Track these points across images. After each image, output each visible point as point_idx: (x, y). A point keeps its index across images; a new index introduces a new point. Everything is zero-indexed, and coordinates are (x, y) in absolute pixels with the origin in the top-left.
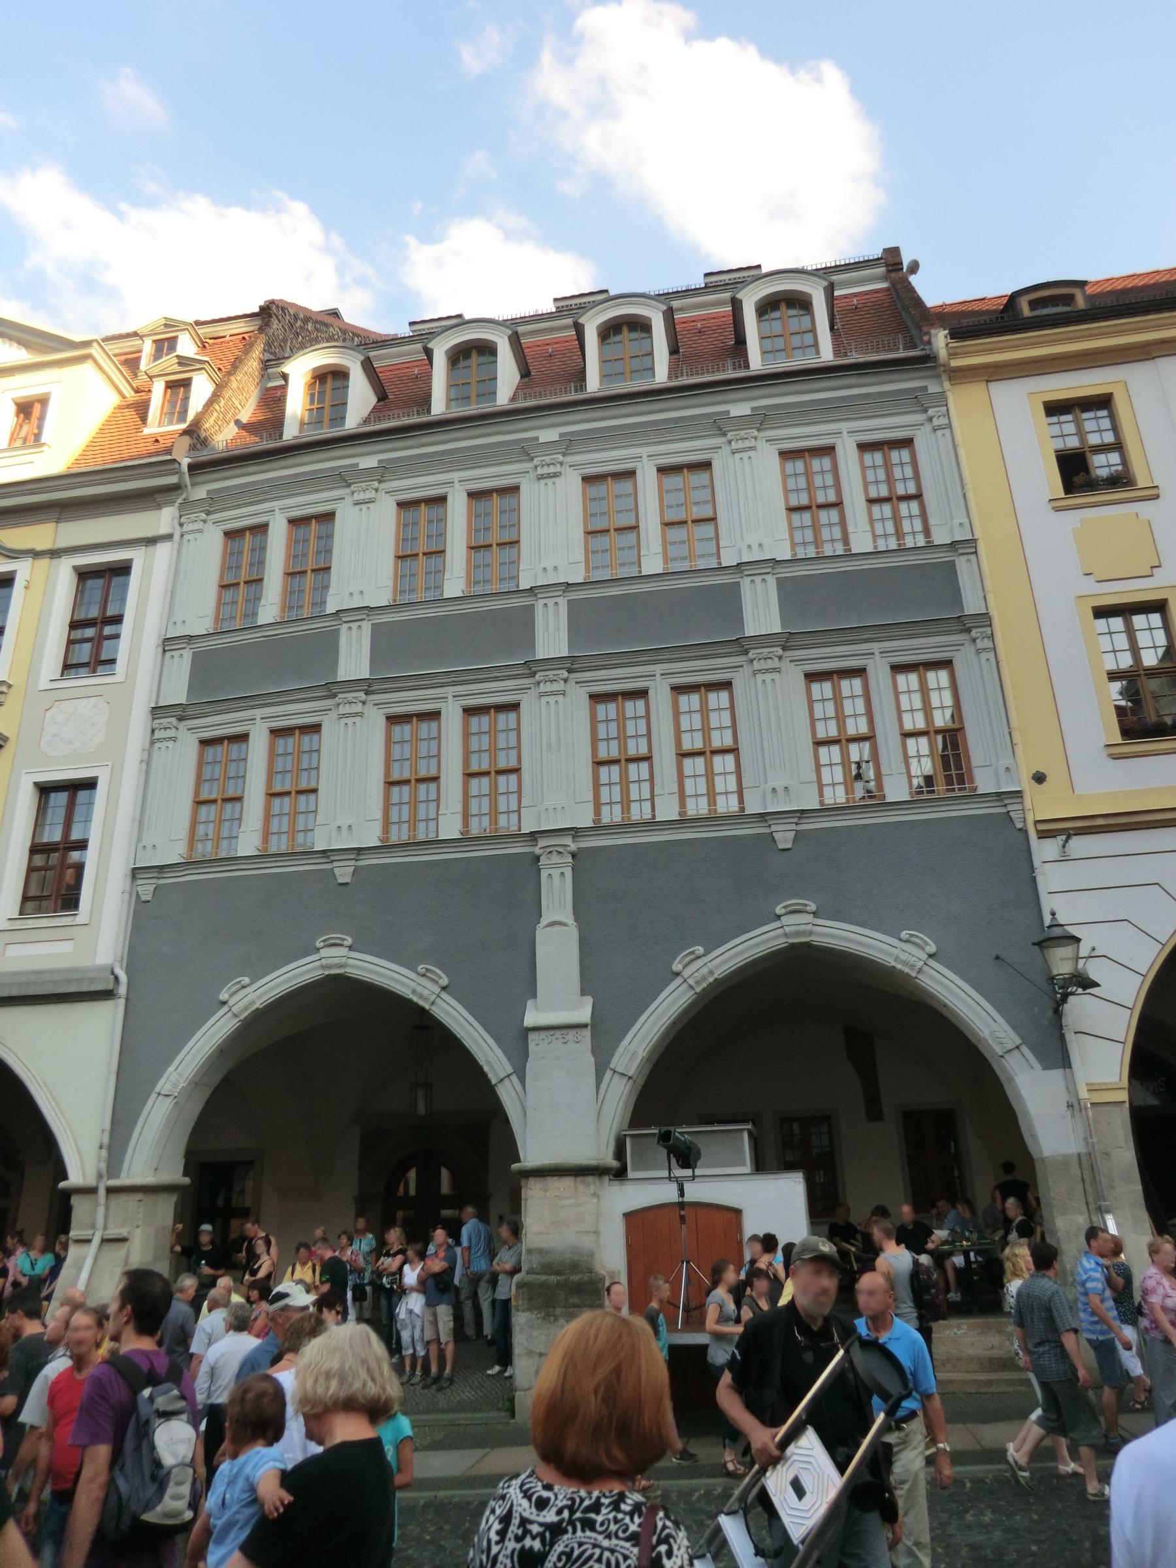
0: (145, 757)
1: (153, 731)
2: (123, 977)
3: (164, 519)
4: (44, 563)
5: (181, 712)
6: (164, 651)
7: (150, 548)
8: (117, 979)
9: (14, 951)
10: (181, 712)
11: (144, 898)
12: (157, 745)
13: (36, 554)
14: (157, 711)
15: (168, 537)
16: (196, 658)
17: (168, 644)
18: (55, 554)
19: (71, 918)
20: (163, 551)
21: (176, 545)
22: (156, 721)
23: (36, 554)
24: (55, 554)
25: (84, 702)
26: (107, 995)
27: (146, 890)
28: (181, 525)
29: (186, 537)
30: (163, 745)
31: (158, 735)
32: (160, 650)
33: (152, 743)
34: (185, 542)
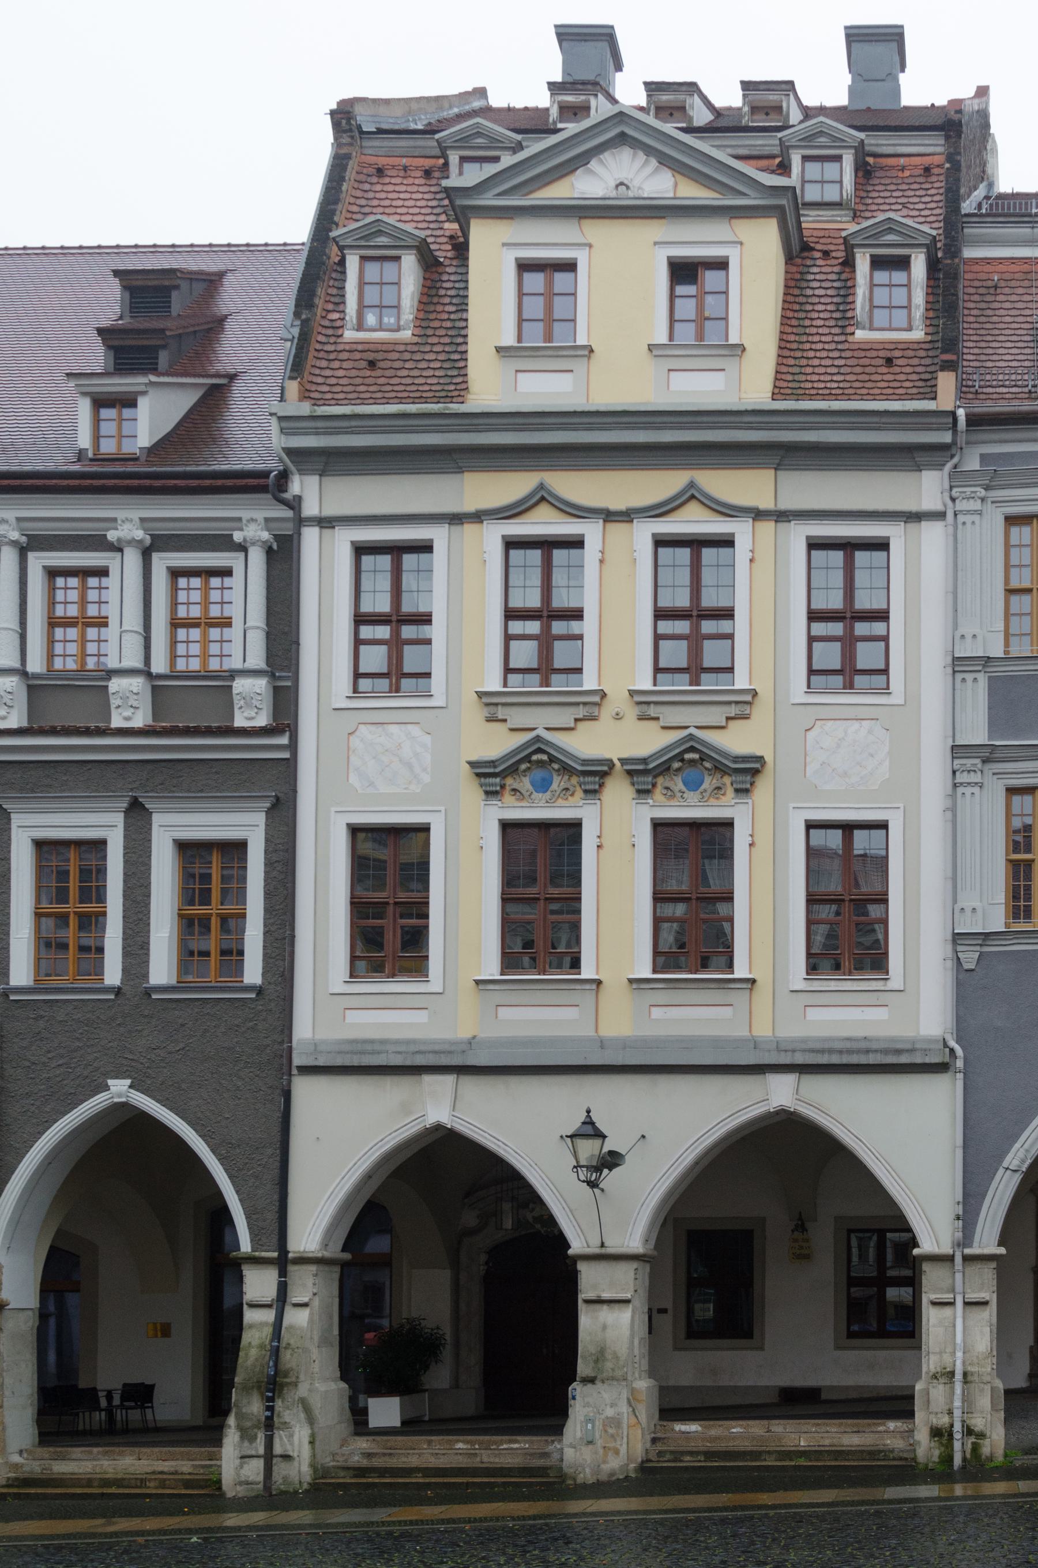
0: (949, 803)
1: (954, 772)
2: (959, 1051)
3: (928, 488)
4: (767, 527)
5: (989, 755)
6: (954, 672)
7: (912, 527)
8: (952, 1050)
9: (813, 1014)
10: (989, 755)
11: (966, 966)
12: (960, 790)
13: (758, 515)
14: (958, 751)
15: (941, 515)
16: (995, 686)
17: (959, 665)
18: (782, 516)
19: (881, 983)
20: (933, 534)
21: (951, 529)
22: (956, 762)
23: (758, 515)
24: (782, 516)
25: (856, 725)
26: (941, 1068)
27: (970, 957)
28: (953, 500)
29: (961, 518)
30: (968, 791)
31: (960, 778)
32: (950, 670)
33: (955, 786)
34: (960, 526)
